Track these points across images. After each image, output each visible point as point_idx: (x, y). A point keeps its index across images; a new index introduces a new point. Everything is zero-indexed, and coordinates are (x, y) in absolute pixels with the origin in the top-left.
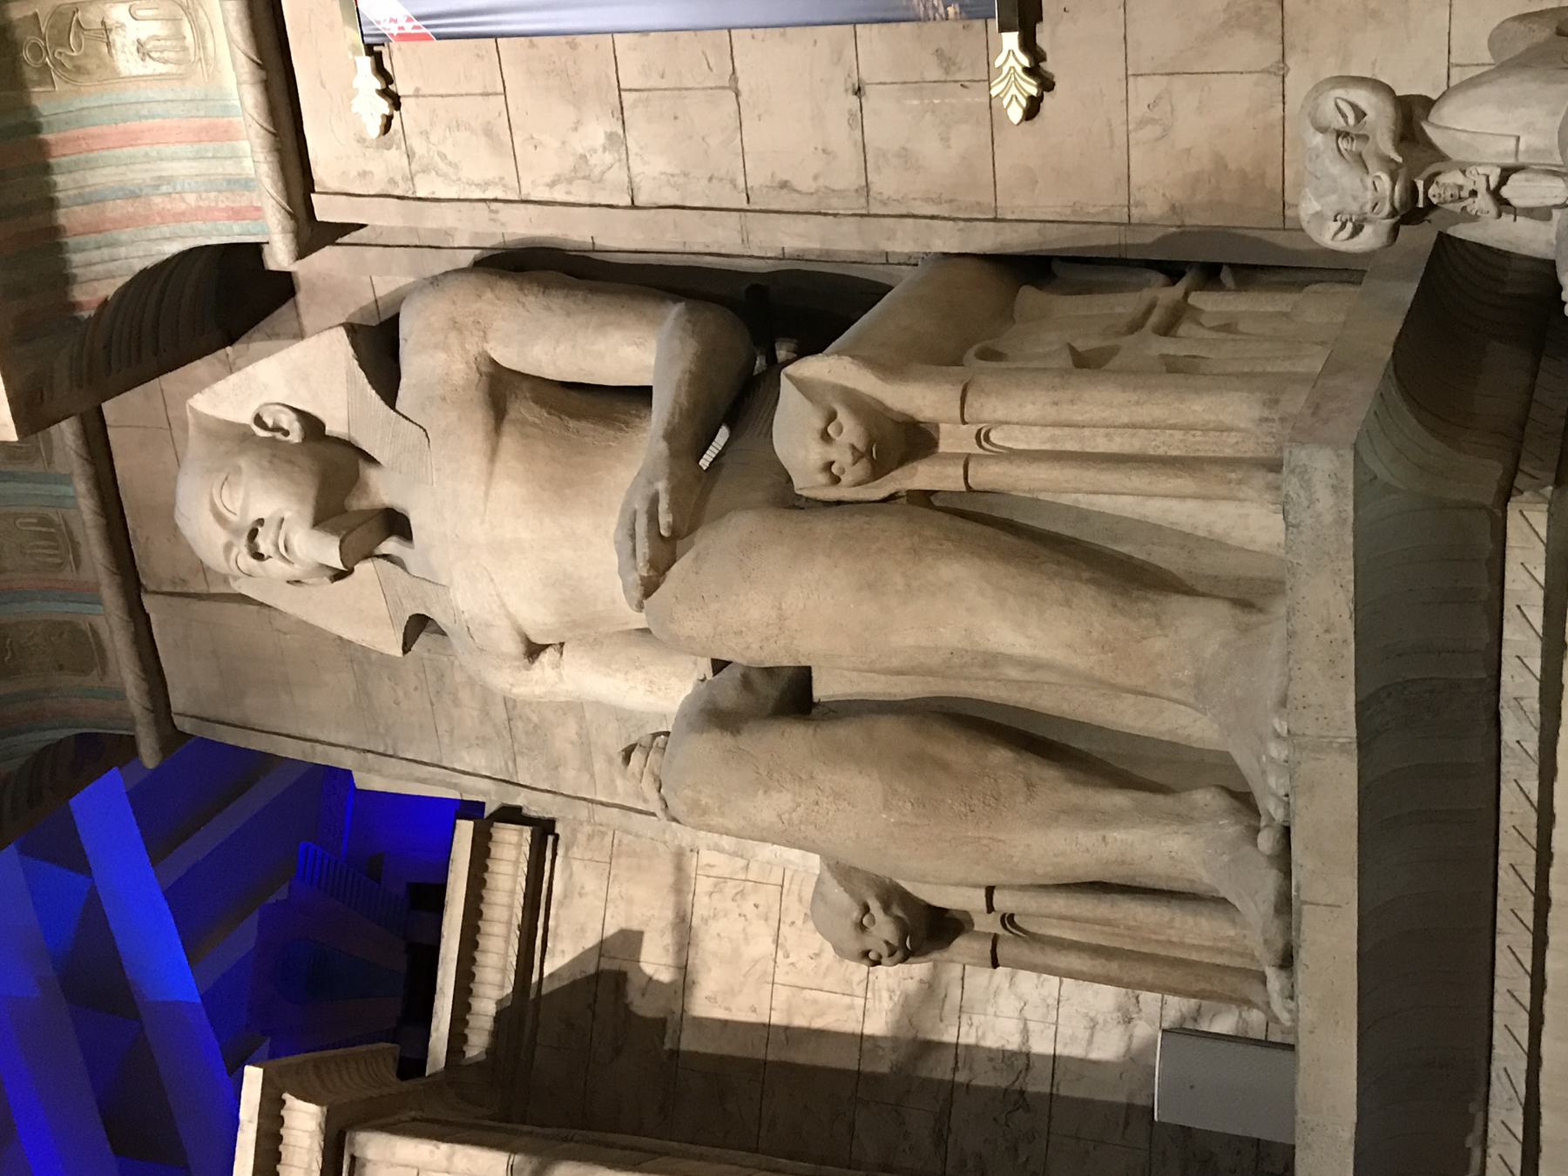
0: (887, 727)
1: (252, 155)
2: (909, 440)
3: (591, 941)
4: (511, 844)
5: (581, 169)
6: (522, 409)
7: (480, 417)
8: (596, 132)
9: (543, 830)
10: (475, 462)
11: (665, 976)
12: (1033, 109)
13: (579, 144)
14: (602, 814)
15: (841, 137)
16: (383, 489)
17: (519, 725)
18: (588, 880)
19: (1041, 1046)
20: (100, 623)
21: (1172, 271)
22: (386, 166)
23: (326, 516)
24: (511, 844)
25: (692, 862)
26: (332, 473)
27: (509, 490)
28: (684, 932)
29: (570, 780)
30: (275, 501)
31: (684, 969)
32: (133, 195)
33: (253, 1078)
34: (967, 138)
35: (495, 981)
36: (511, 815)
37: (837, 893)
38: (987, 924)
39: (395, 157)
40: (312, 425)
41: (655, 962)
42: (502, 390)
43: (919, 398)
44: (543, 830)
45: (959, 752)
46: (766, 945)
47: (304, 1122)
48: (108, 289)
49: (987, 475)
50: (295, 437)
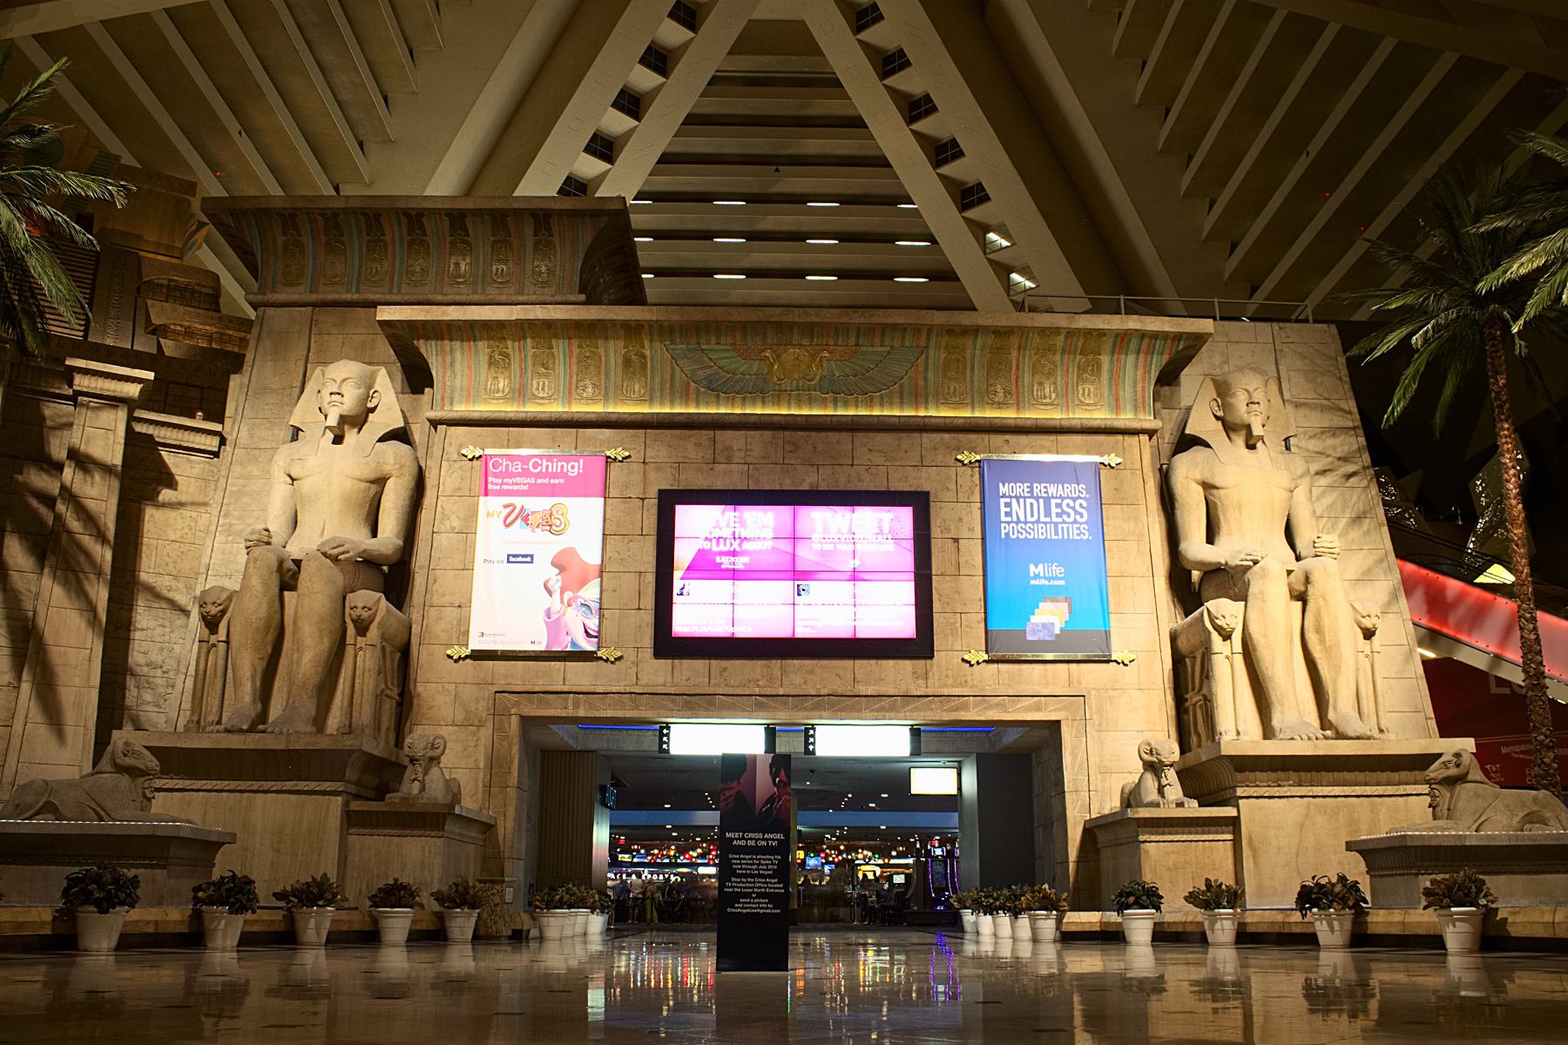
0: (278, 616)
1: (461, 409)
2: (362, 628)
3: (174, 470)
4: (212, 443)
5: (445, 517)
6: (374, 488)
7: (372, 476)
8: (456, 524)
9: (216, 455)
10: (358, 474)
11: (161, 498)
12: (450, 657)
13: (453, 517)
14: (223, 480)
15: (447, 600)
16: (351, 436)
17: (257, 453)
18: (196, 471)
19: (137, 635)
20: (302, 289)
21: (401, 694)
22: (452, 451)
23: (344, 420)
24: (212, 443)
25: (202, 509)
26: (357, 420)
27: (349, 484)
28: (181, 505)
29: (236, 469)
30: (349, 402)
31: (163, 505)
32: (452, 364)
33: (150, 375)
34: (443, 637)
35: (161, 434)
36: (223, 442)
37: (224, 596)
38: (213, 639)
39: (455, 456)
40: (373, 410)
41: (166, 495)
42: (380, 482)
43: (373, 633)
44: (216, 455)
45: (270, 638)
46: (172, 537)
47: (133, 390)
48: (423, 351)
49: (350, 651)
50: (370, 405)
